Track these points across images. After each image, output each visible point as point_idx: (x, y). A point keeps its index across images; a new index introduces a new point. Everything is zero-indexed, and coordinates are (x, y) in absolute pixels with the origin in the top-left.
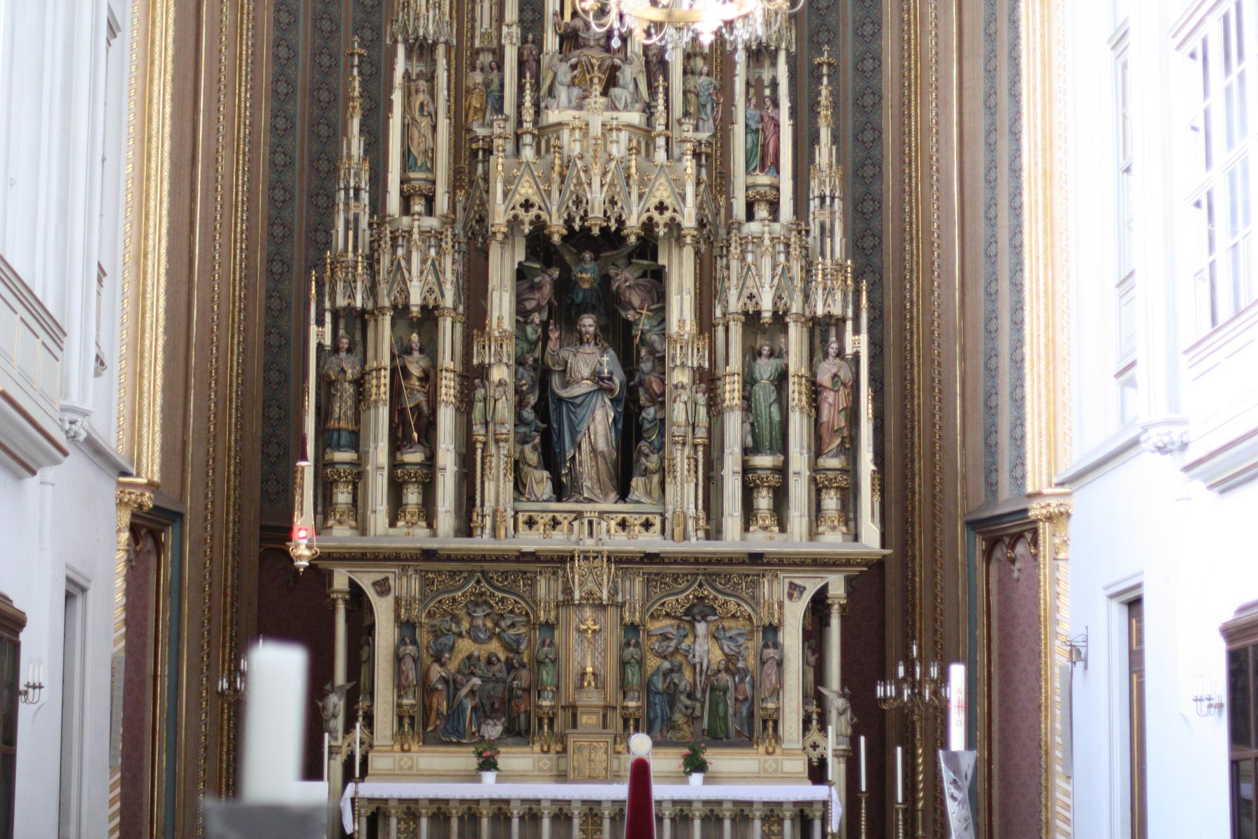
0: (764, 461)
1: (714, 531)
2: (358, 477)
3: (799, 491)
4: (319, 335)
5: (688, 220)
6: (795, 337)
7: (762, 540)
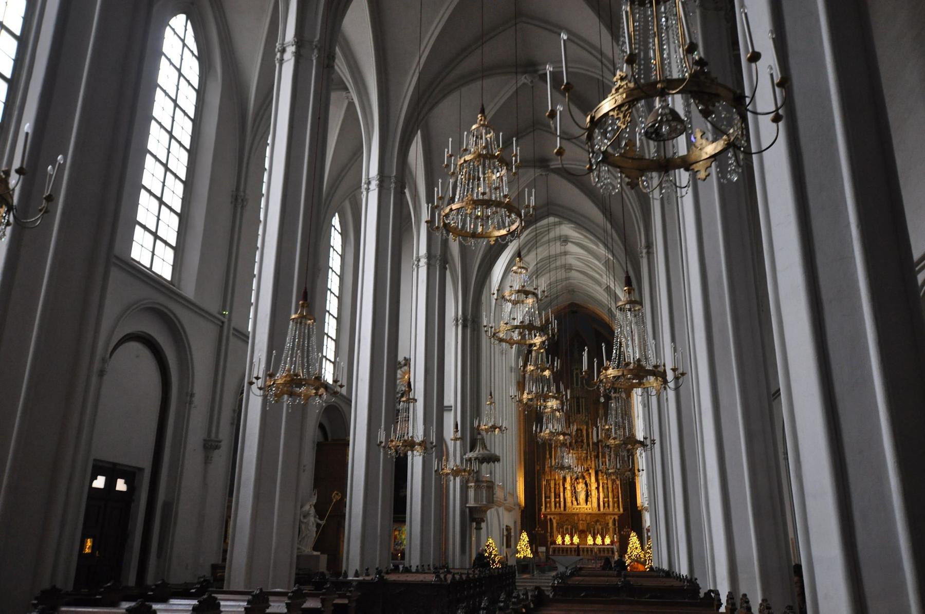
2: (550, 502)
4: (544, 483)
5: (593, 466)
7: (607, 511)
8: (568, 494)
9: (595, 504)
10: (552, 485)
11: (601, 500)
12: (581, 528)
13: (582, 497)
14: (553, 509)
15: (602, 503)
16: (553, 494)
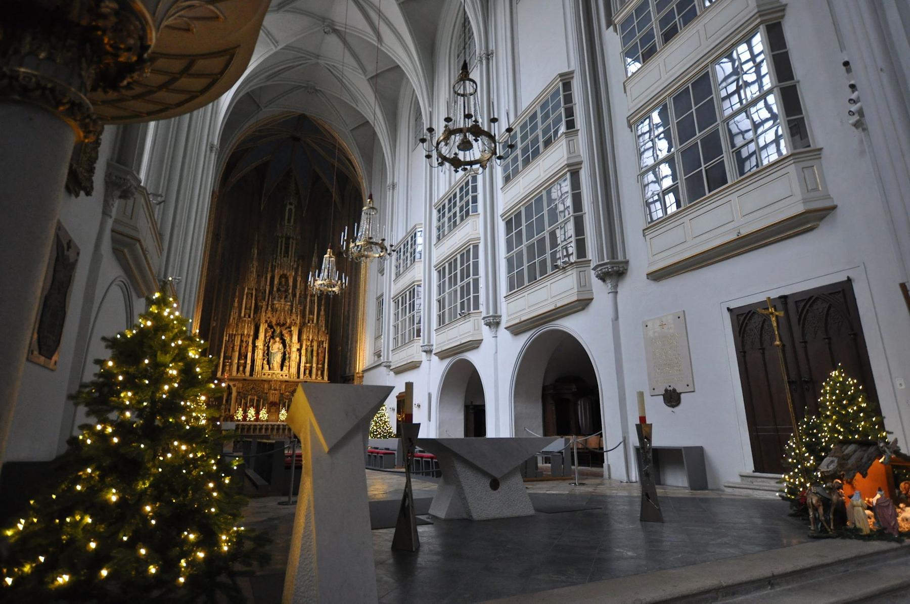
0: (308, 365)
1: (298, 377)
2: (231, 364)
3: (314, 370)
4: (225, 338)
5: (298, 322)
6: (315, 344)
7: (308, 379)
8: (259, 354)
9: (294, 370)
10: (237, 342)
11: (302, 365)
12: (271, 399)
13: (277, 359)
14: (234, 373)
15: (302, 369)
16: (237, 354)
